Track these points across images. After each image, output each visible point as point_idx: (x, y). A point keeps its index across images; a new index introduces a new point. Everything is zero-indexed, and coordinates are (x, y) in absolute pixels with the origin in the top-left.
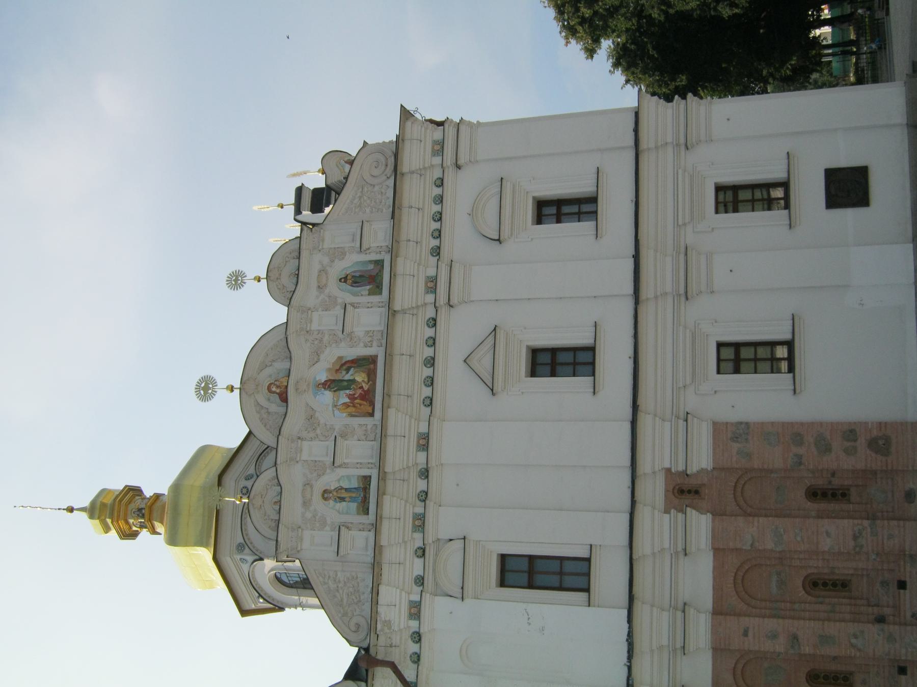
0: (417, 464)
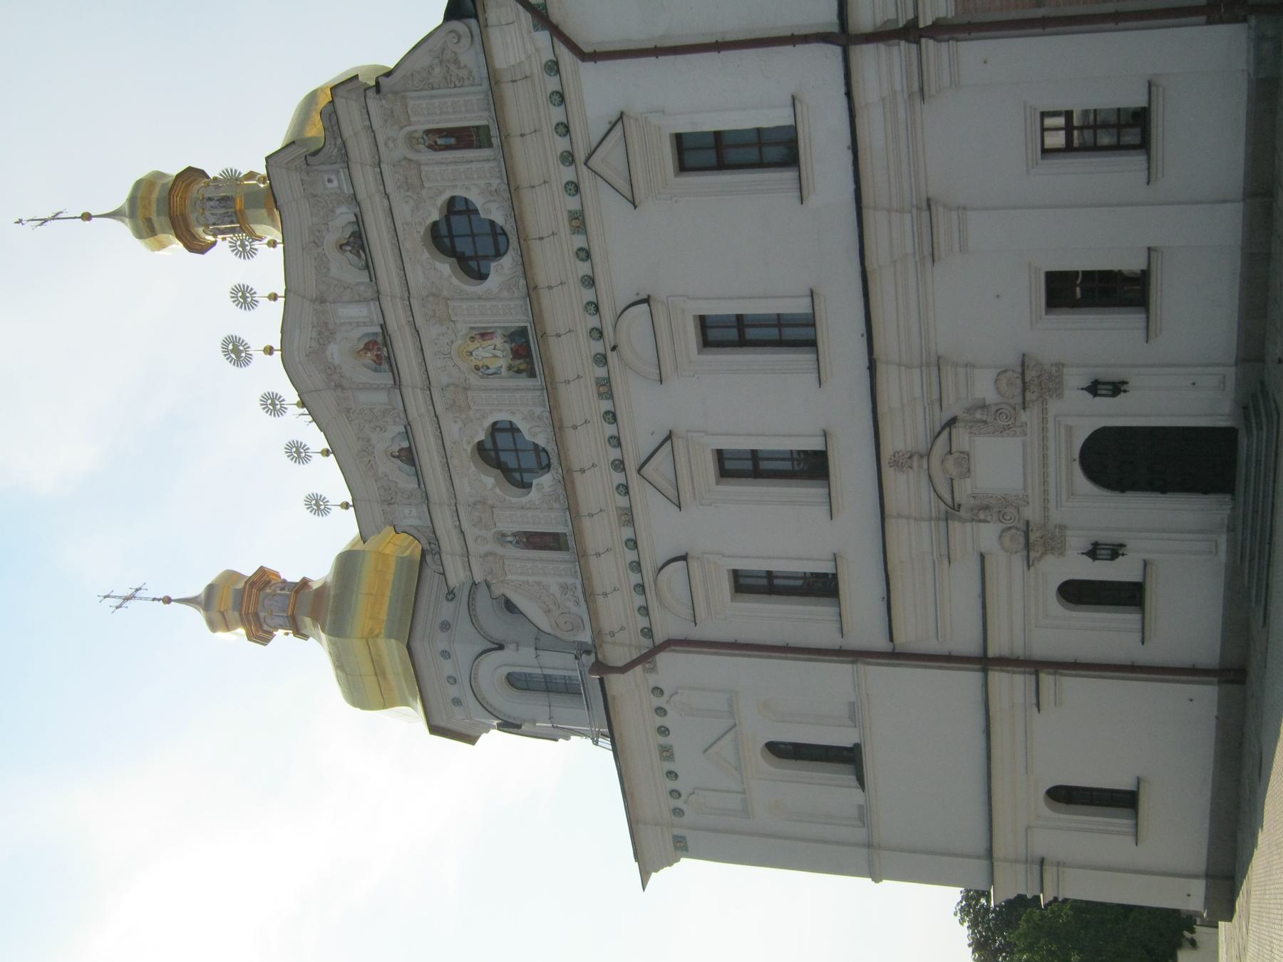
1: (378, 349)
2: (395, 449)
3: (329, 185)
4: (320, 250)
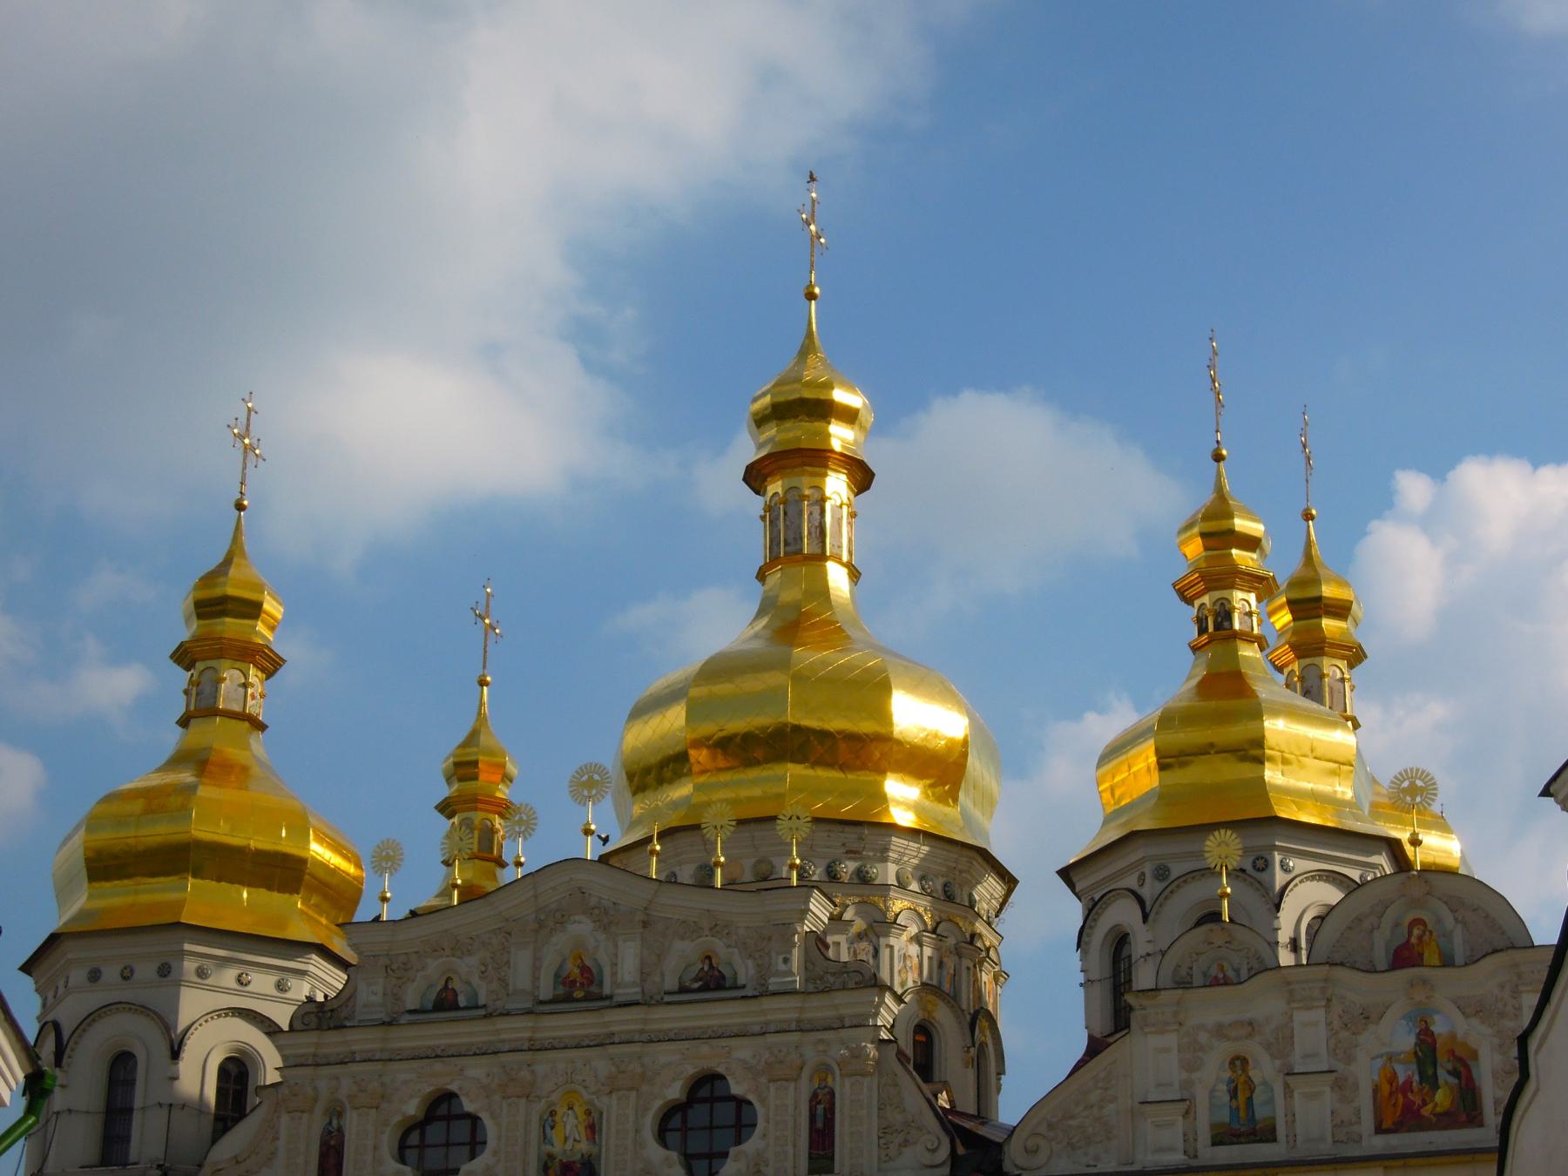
1: (582, 984)
2: (456, 984)
3: (780, 958)
4: (707, 932)
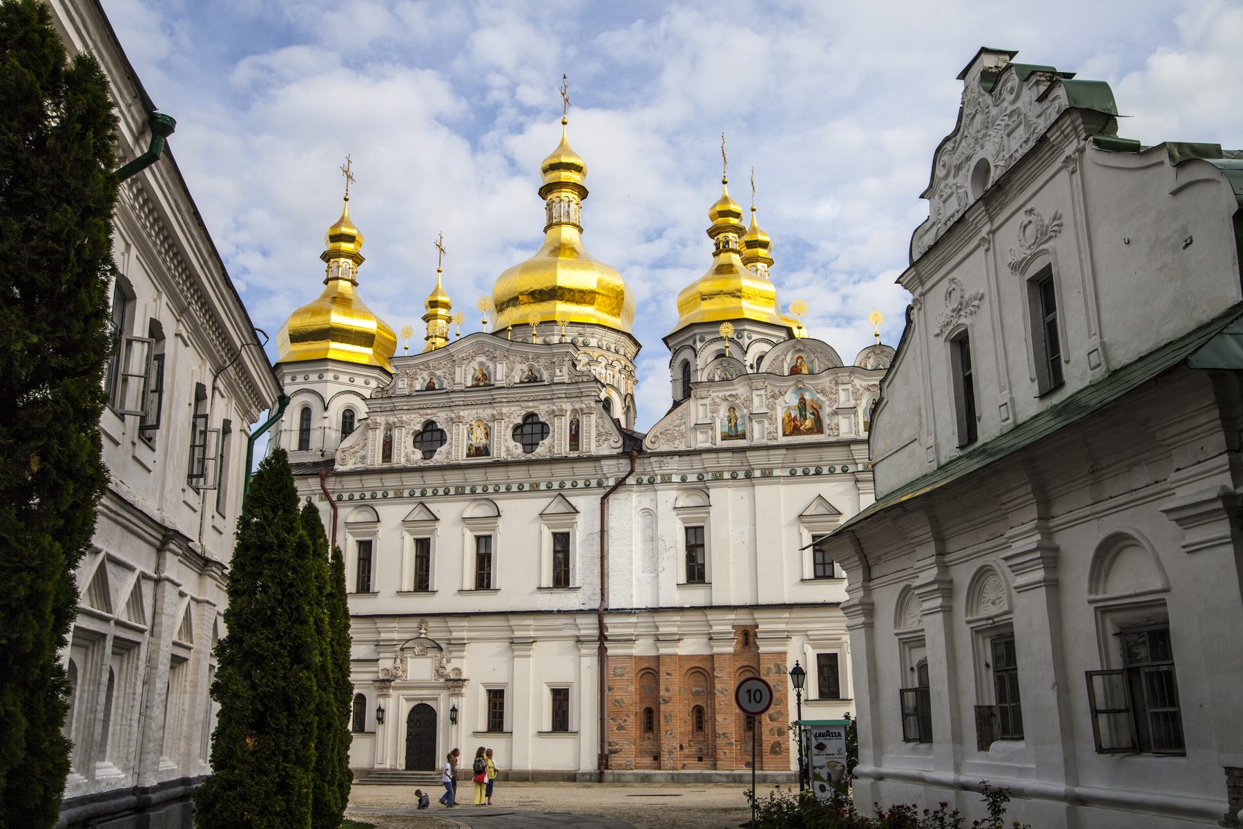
0: (753, 470)
2: (435, 381)
